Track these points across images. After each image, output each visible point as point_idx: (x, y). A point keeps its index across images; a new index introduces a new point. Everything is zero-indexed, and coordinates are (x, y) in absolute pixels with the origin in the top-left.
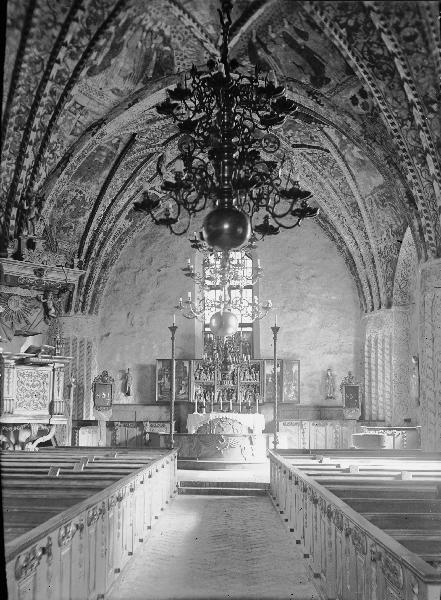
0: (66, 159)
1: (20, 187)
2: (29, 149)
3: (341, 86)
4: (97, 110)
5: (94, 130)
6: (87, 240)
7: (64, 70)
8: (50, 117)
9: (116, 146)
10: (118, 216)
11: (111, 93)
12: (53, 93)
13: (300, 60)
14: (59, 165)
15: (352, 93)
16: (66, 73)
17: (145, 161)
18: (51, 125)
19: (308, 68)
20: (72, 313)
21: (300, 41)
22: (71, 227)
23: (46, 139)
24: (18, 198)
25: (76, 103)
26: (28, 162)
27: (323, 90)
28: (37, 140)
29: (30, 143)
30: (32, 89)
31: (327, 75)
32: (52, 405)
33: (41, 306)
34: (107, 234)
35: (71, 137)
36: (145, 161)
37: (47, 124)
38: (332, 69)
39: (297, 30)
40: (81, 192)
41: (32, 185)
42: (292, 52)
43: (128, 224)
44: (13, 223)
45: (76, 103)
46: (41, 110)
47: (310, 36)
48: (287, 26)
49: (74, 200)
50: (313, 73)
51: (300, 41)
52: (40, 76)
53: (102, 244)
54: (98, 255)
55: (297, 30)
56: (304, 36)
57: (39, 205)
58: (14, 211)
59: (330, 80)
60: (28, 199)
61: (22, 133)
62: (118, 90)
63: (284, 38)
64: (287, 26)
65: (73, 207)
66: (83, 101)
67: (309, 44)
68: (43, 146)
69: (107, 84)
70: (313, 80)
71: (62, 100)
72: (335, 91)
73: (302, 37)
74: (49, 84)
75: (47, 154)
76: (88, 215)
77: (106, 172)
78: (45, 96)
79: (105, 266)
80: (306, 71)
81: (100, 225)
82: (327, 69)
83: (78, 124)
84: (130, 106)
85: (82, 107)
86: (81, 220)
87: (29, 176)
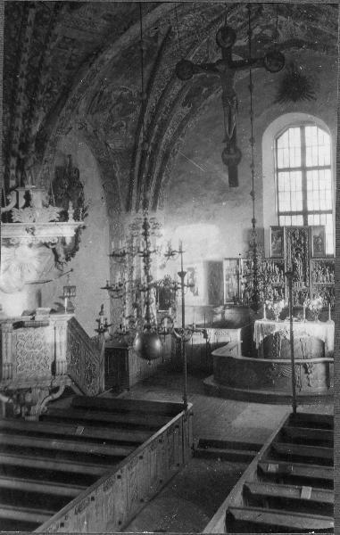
0: (66, 92)
1: (16, 136)
2: (20, 96)
4: (90, 39)
5: (91, 59)
6: (142, 134)
7: (43, 11)
8: (39, 58)
9: (156, 38)
10: (173, 105)
11: (102, 21)
12: (35, 34)
14: (58, 102)
16: (46, 13)
17: (191, 48)
18: (40, 64)
20: (133, 212)
22: (123, 125)
23: (37, 81)
24: (15, 147)
25: (65, 37)
26: (20, 109)
28: (28, 85)
29: (21, 90)
30: (13, 36)
32: (54, 365)
33: (51, 251)
34: (164, 125)
35: (67, 72)
36: (191, 48)
37: (37, 66)
40: (125, 90)
41: (30, 129)
43: (187, 110)
44: (13, 172)
45: (65, 37)
46: (25, 56)
49: (120, 99)
52: (18, 22)
53: (159, 136)
54: (156, 147)
57: (40, 148)
58: (13, 161)
60: (24, 147)
61: (11, 80)
62: (110, 15)
65: (120, 106)
66: (74, 34)
68: (36, 88)
69: (96, 12)
71: (47, 41)
74: (29, 29)
75: (40, 97)
76: (138, 109)
77: (149, 67)
78: (27, 41)
79: (166, 157)
81: (153, 117)
83: (74, 58)
84: (125, 30)
85: (73, 40)
86: (131, 116)
87: (26, 121)
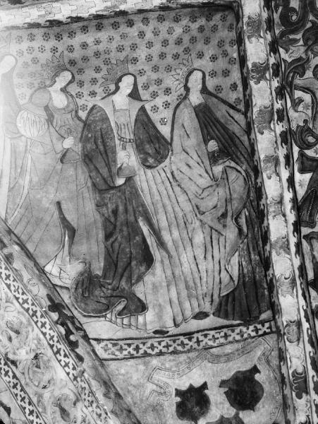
3: (174, 341)
13: (85, 211)
15: (195, 378)
19: (93, 249)
21: (127, 157)
27: (99, 328)
31: (140, 291)
38: (173, 280)
39: (144, 122)
42: (78, 176)
47: (175, 161)
48: (121, 99)
50: (98, 268)
51: (127, 157)
55: (144, 122)
56: (153, 145)
59: (143, 307)
63: (86, 125)
64: (121, 99)
67: (150, 183)
70: (87, 284)
72: (138, 350)
73: (140, 148)
80: (82, 248)
82: (158, 274)
